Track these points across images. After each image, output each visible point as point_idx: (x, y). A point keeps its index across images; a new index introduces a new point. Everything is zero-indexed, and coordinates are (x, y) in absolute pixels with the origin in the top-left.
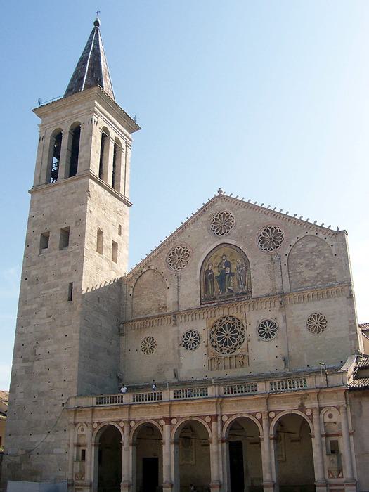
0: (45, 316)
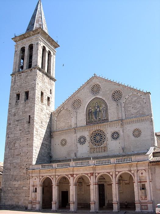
0: (18, 129)
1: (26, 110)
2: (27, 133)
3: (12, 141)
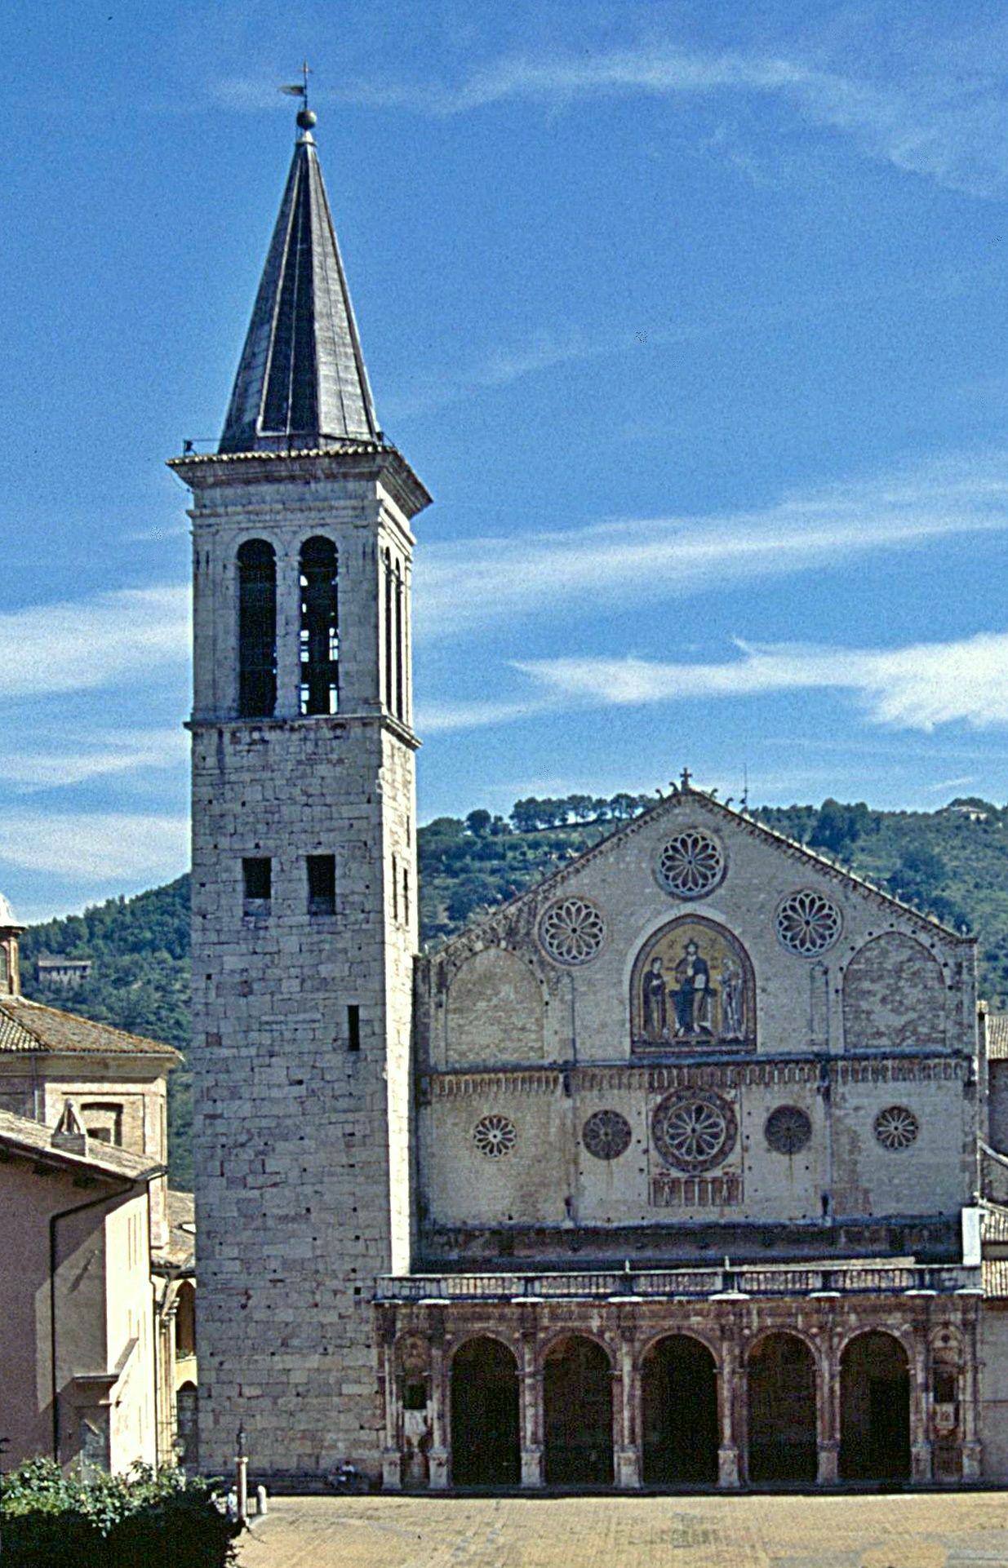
0: (280, 1075)
1: (324, 970)
2: (343, 1103)
3: (243, 1138)
